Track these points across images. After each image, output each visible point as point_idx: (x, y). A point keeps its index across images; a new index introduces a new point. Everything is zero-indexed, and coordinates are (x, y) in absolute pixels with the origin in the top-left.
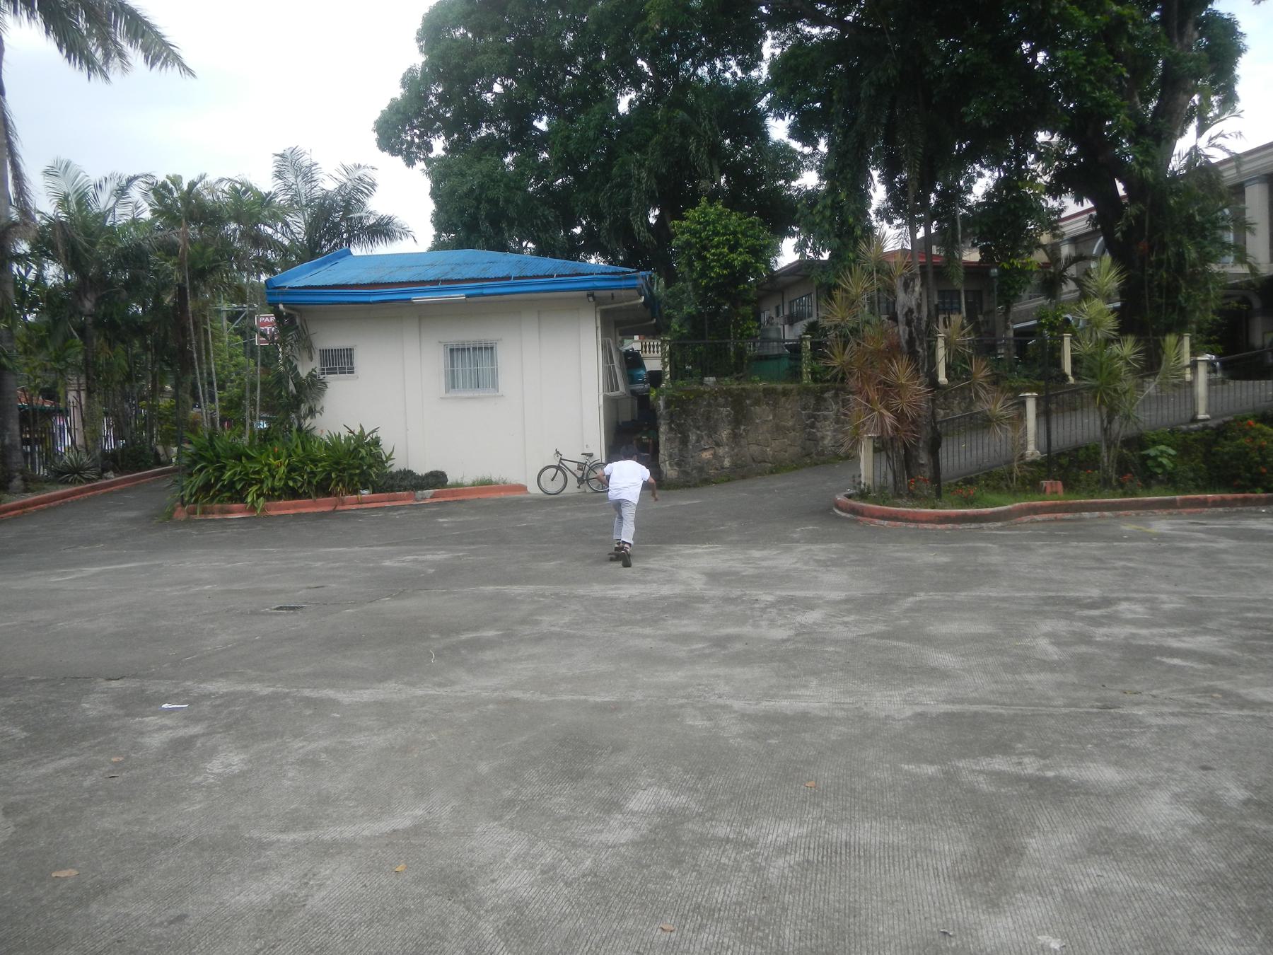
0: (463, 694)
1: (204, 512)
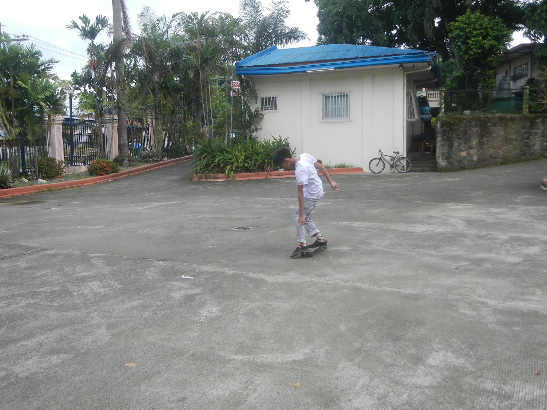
0: (331, 282)
1: (206, 178)
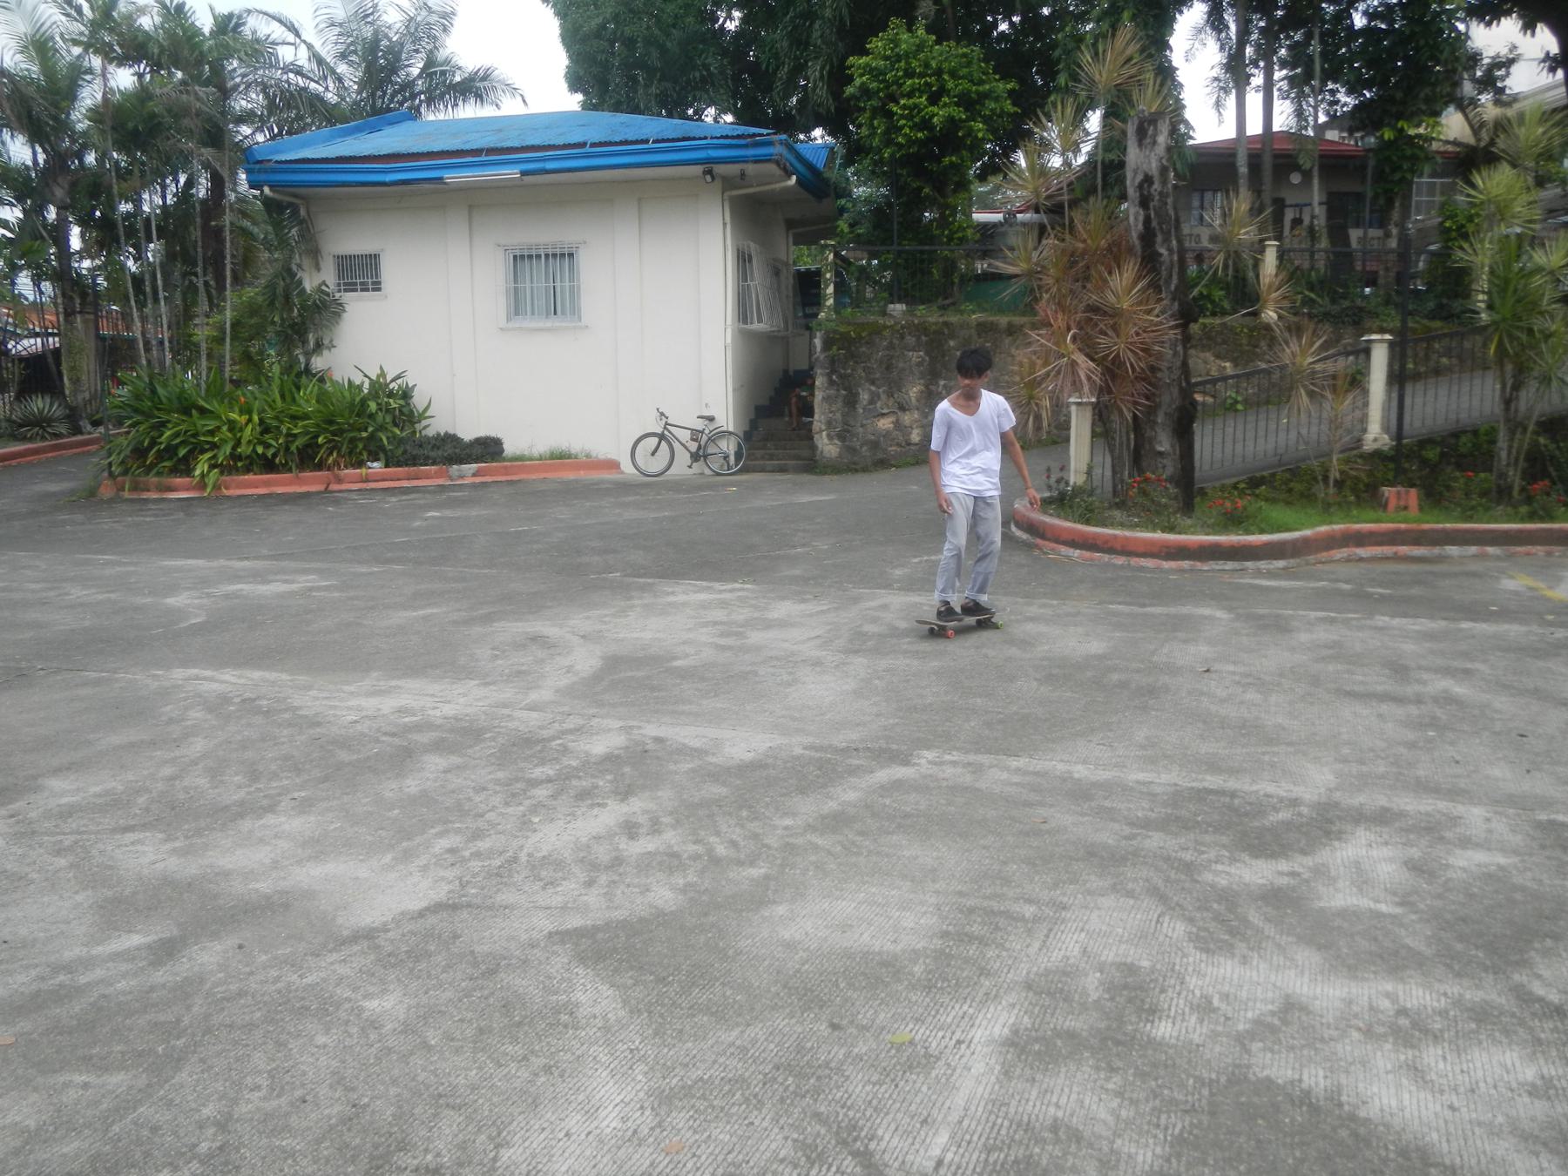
1: (135, 488)
